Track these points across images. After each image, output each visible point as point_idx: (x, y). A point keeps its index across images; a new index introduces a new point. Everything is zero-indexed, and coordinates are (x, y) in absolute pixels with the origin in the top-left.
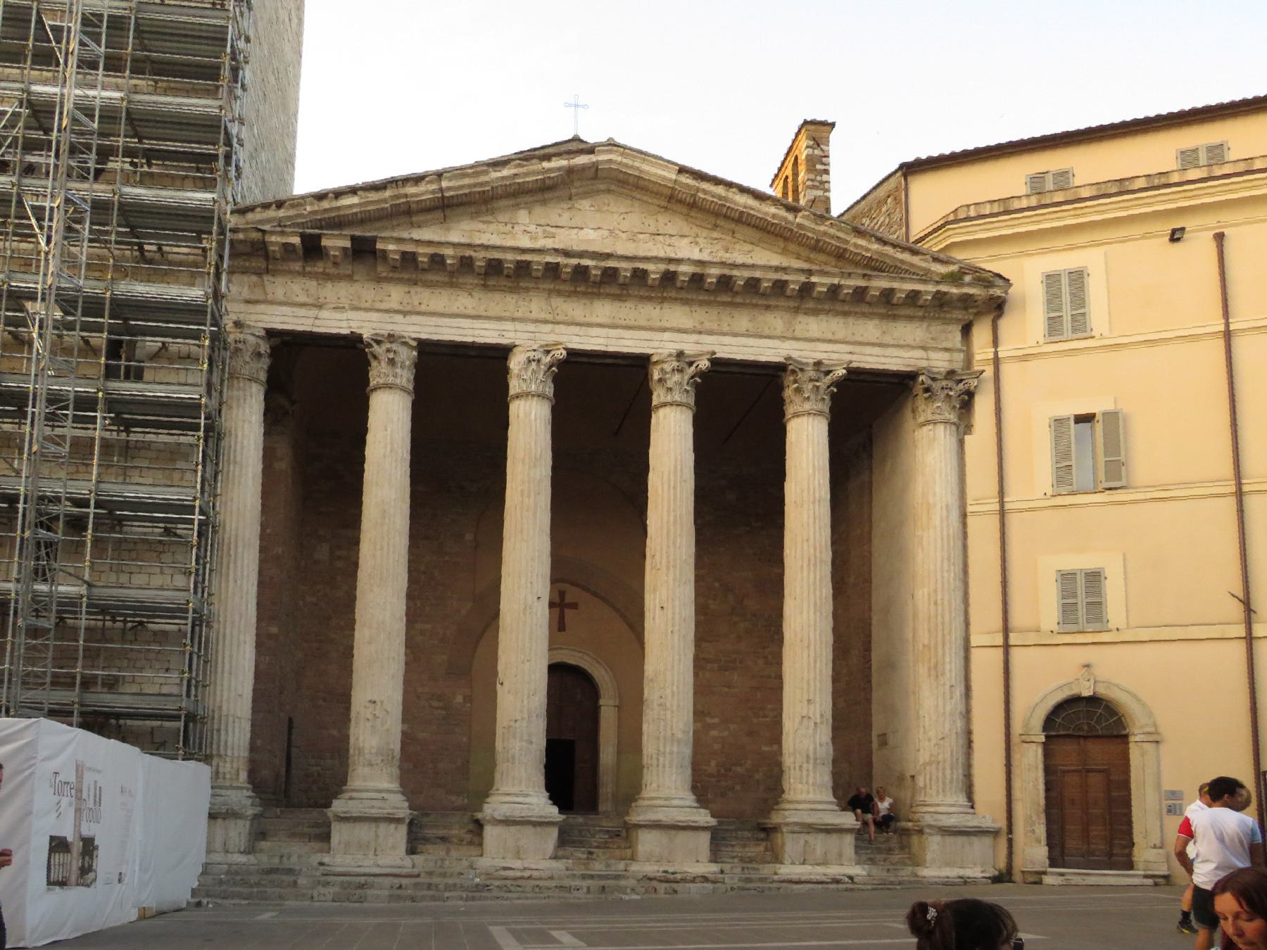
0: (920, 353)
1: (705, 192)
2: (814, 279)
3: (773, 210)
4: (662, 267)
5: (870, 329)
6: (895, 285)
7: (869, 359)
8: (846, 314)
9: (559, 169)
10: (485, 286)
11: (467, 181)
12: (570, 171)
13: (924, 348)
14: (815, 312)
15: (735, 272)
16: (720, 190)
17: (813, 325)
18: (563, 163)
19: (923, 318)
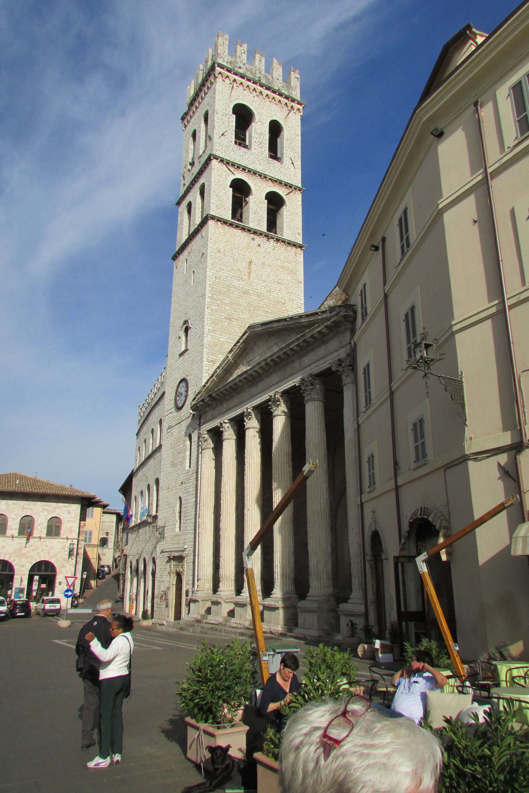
0: (336, 354)
1: (268, 328)
2: (291, 347)
3: (281, 324)
4: (258, 367)
5: (321, 351)
6: (312, 333)
7: (321, 366)
8: (313, 350)
9: (242, 343)
10: (237, 393)
11: (226, 361)
12: (244, 342)
13: (336, 351)
14: (305, 355)
15: (273, 357)
16: (270, 326)
17: (306, 360)
18: (241, 341)
19: (335, 336)
